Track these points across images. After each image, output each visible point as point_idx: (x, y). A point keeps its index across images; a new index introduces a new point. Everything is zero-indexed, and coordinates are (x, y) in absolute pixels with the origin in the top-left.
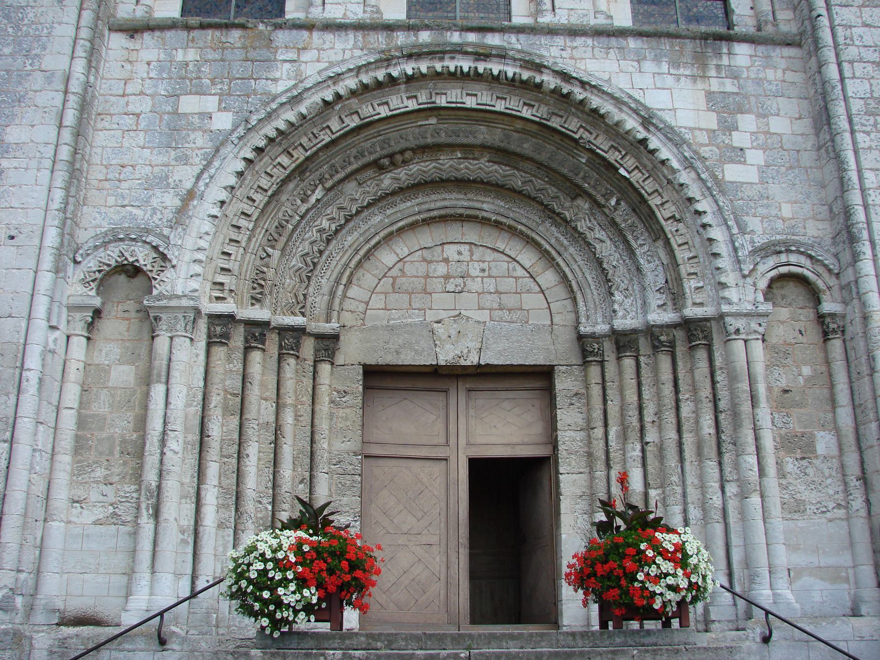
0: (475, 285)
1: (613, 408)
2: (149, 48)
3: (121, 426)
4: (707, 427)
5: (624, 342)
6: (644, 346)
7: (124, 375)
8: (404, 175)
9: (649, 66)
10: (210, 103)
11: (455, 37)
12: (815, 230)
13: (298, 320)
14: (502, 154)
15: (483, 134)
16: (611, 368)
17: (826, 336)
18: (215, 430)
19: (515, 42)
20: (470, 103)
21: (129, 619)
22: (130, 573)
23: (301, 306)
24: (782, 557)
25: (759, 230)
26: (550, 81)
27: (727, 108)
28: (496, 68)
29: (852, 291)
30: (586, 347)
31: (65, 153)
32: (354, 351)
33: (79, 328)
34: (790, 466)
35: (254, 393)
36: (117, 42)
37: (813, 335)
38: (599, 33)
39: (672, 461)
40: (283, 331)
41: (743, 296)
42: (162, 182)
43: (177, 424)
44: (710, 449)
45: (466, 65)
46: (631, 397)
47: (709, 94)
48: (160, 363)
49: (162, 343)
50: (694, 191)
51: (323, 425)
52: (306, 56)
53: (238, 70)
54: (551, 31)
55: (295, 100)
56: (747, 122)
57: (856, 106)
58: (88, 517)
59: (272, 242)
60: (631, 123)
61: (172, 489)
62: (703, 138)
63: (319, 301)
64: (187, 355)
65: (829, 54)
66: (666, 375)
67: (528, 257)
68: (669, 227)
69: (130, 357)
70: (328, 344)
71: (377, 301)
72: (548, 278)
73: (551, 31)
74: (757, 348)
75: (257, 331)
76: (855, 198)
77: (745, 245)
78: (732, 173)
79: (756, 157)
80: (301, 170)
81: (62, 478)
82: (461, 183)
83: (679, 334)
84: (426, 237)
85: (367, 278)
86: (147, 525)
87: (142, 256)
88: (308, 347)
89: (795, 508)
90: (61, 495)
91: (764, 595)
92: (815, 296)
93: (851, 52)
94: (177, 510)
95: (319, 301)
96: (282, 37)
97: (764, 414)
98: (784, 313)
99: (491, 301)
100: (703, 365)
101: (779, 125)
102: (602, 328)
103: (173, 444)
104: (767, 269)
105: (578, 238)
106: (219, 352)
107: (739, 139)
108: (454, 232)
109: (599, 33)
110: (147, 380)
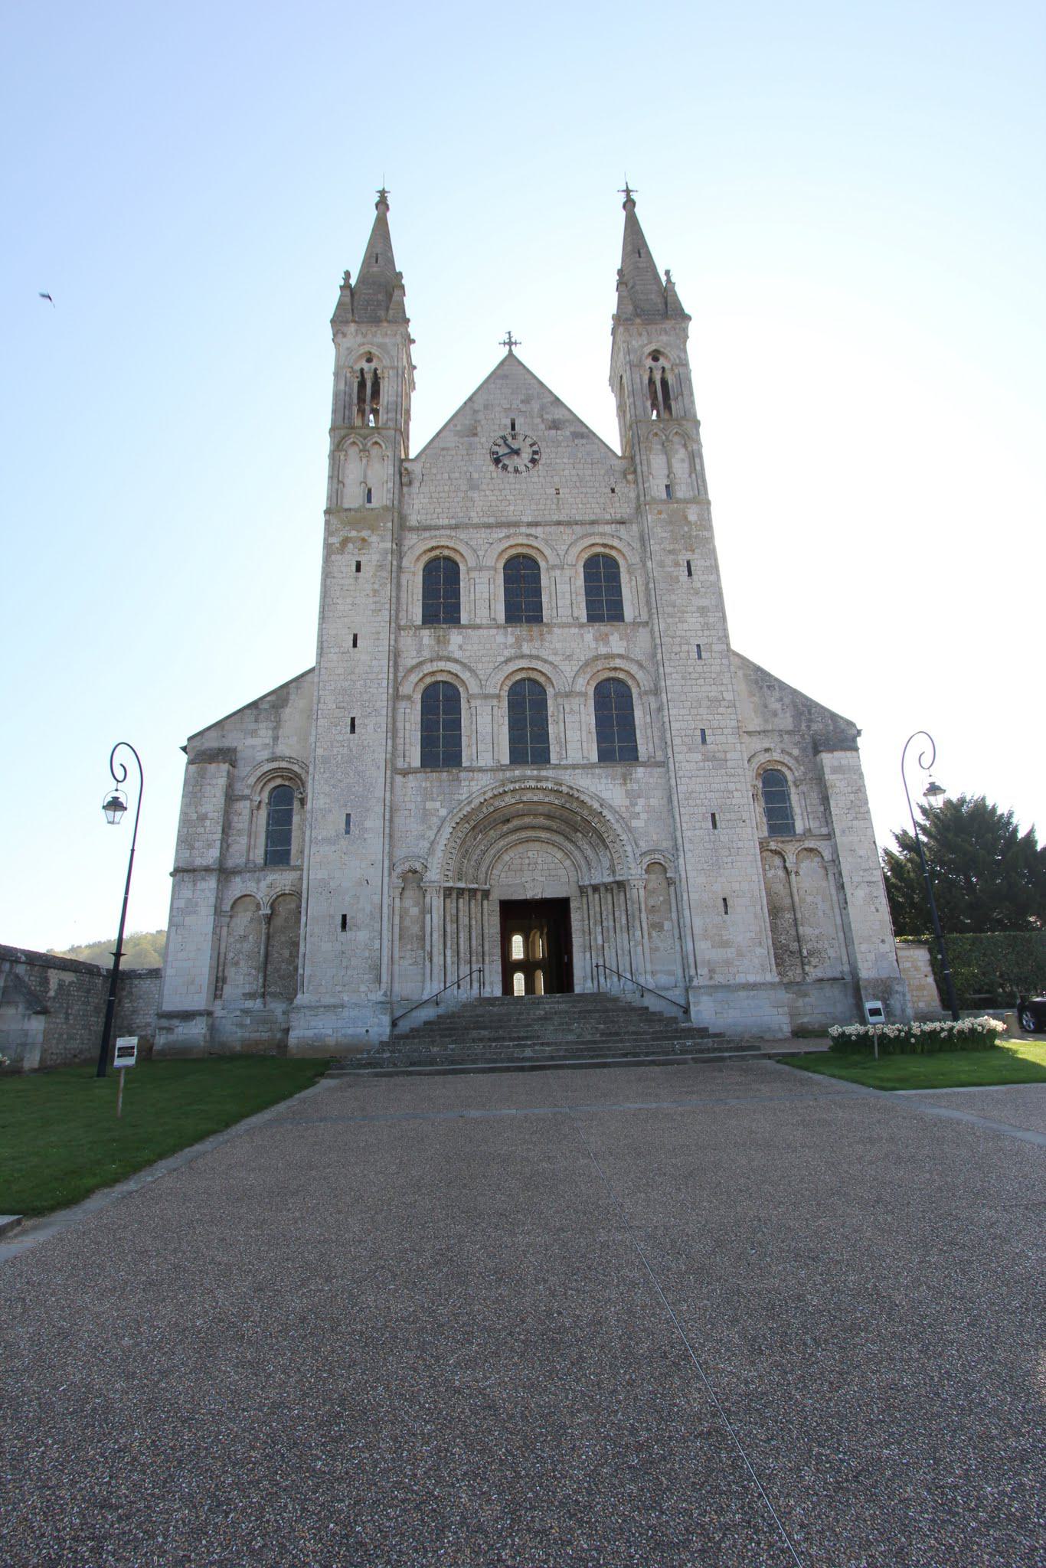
0: (540, 867)
1: (592, 913)
2: (412, 781)
3: (415, 929)
4: (624, 921)
5: (596, 888)
6: (602, 889)
7: (414, 911)
8: (510, 825)
9: (603, 781)
10: (438, 804)
11: (529, 773)
12: (666, 844)
13: (475, 886)
14: (548, 816)
15: (541, 809)
16: (591, 898)
17: (669, 885)
18: (448, 929)
19: (550, 773)
20: (535, 799)
21: (425, 997)
22: (423, 982)
23: (476, 880)
24: (649, 967)
25: (644, 846)
26: (565, 789)
28: (544, 785)
29: (677, 869)
30: (582, 890)
31: (387, 830)
32: (496, 895)
33: (397, 894)
34: (654, 934)
35: (461, 914)
36: (399, 778)
37: (665, 884)
38: (584, 767)
39: (612, 933)
40: (470, 890)
41: (633, 871)
42: (423, 837)
43: (435, 928)
44: (625, 930)
45: (533, 784)
46: (598, 909)
48: (428, 906)
49: (428, 899)
50: (620, 831)
51: (486, 924)
53: (447, 790)
54: (566, 767)
55: (470, 803)
56: (641, 801)
58: (406, 963)
59: (464, 857)
60: (596, 806)
61: (435, 950)
63: (482, 876)
64: (436, 902)
65: (672, 774)
66: (610, 901)
67: (559, 855)
68: (610, 845)
69: (417, 904)
70: (486, 894)
71: (503, 875)
72: (568, 863)
73: (566, 767)
74: (642, 892)
75: (461, 892)
76: (678, 834)
77: (638, 852)
78: (635, 823)
79: (644, 816)
80: (474, 828)
81: (396, 949)
82: (533, 828)
83: (615, 886)
84: (521, 848)
85: (499, 866)
86: (427, 963)
87: (418, 866)
88: (479, 896)
89: (654, 950)
90: (396, 956)
91: (642, 981)
92: (665, 870)
93: (680, 774)
94: (438, 959)
95: (482, 876)
96: (463, 775)
97: (644, 915)
98: (653, 877)
99: (546, 873)
100: (622, 898)
101: (654, 802)
102: (587, 883)
103: (435, 936)
104: (647, 860)
105: (578, 848)
106: (448, 901)
107: (638, 809)
108: (531, 844)
109: (584, 767)
110: (423, 912)
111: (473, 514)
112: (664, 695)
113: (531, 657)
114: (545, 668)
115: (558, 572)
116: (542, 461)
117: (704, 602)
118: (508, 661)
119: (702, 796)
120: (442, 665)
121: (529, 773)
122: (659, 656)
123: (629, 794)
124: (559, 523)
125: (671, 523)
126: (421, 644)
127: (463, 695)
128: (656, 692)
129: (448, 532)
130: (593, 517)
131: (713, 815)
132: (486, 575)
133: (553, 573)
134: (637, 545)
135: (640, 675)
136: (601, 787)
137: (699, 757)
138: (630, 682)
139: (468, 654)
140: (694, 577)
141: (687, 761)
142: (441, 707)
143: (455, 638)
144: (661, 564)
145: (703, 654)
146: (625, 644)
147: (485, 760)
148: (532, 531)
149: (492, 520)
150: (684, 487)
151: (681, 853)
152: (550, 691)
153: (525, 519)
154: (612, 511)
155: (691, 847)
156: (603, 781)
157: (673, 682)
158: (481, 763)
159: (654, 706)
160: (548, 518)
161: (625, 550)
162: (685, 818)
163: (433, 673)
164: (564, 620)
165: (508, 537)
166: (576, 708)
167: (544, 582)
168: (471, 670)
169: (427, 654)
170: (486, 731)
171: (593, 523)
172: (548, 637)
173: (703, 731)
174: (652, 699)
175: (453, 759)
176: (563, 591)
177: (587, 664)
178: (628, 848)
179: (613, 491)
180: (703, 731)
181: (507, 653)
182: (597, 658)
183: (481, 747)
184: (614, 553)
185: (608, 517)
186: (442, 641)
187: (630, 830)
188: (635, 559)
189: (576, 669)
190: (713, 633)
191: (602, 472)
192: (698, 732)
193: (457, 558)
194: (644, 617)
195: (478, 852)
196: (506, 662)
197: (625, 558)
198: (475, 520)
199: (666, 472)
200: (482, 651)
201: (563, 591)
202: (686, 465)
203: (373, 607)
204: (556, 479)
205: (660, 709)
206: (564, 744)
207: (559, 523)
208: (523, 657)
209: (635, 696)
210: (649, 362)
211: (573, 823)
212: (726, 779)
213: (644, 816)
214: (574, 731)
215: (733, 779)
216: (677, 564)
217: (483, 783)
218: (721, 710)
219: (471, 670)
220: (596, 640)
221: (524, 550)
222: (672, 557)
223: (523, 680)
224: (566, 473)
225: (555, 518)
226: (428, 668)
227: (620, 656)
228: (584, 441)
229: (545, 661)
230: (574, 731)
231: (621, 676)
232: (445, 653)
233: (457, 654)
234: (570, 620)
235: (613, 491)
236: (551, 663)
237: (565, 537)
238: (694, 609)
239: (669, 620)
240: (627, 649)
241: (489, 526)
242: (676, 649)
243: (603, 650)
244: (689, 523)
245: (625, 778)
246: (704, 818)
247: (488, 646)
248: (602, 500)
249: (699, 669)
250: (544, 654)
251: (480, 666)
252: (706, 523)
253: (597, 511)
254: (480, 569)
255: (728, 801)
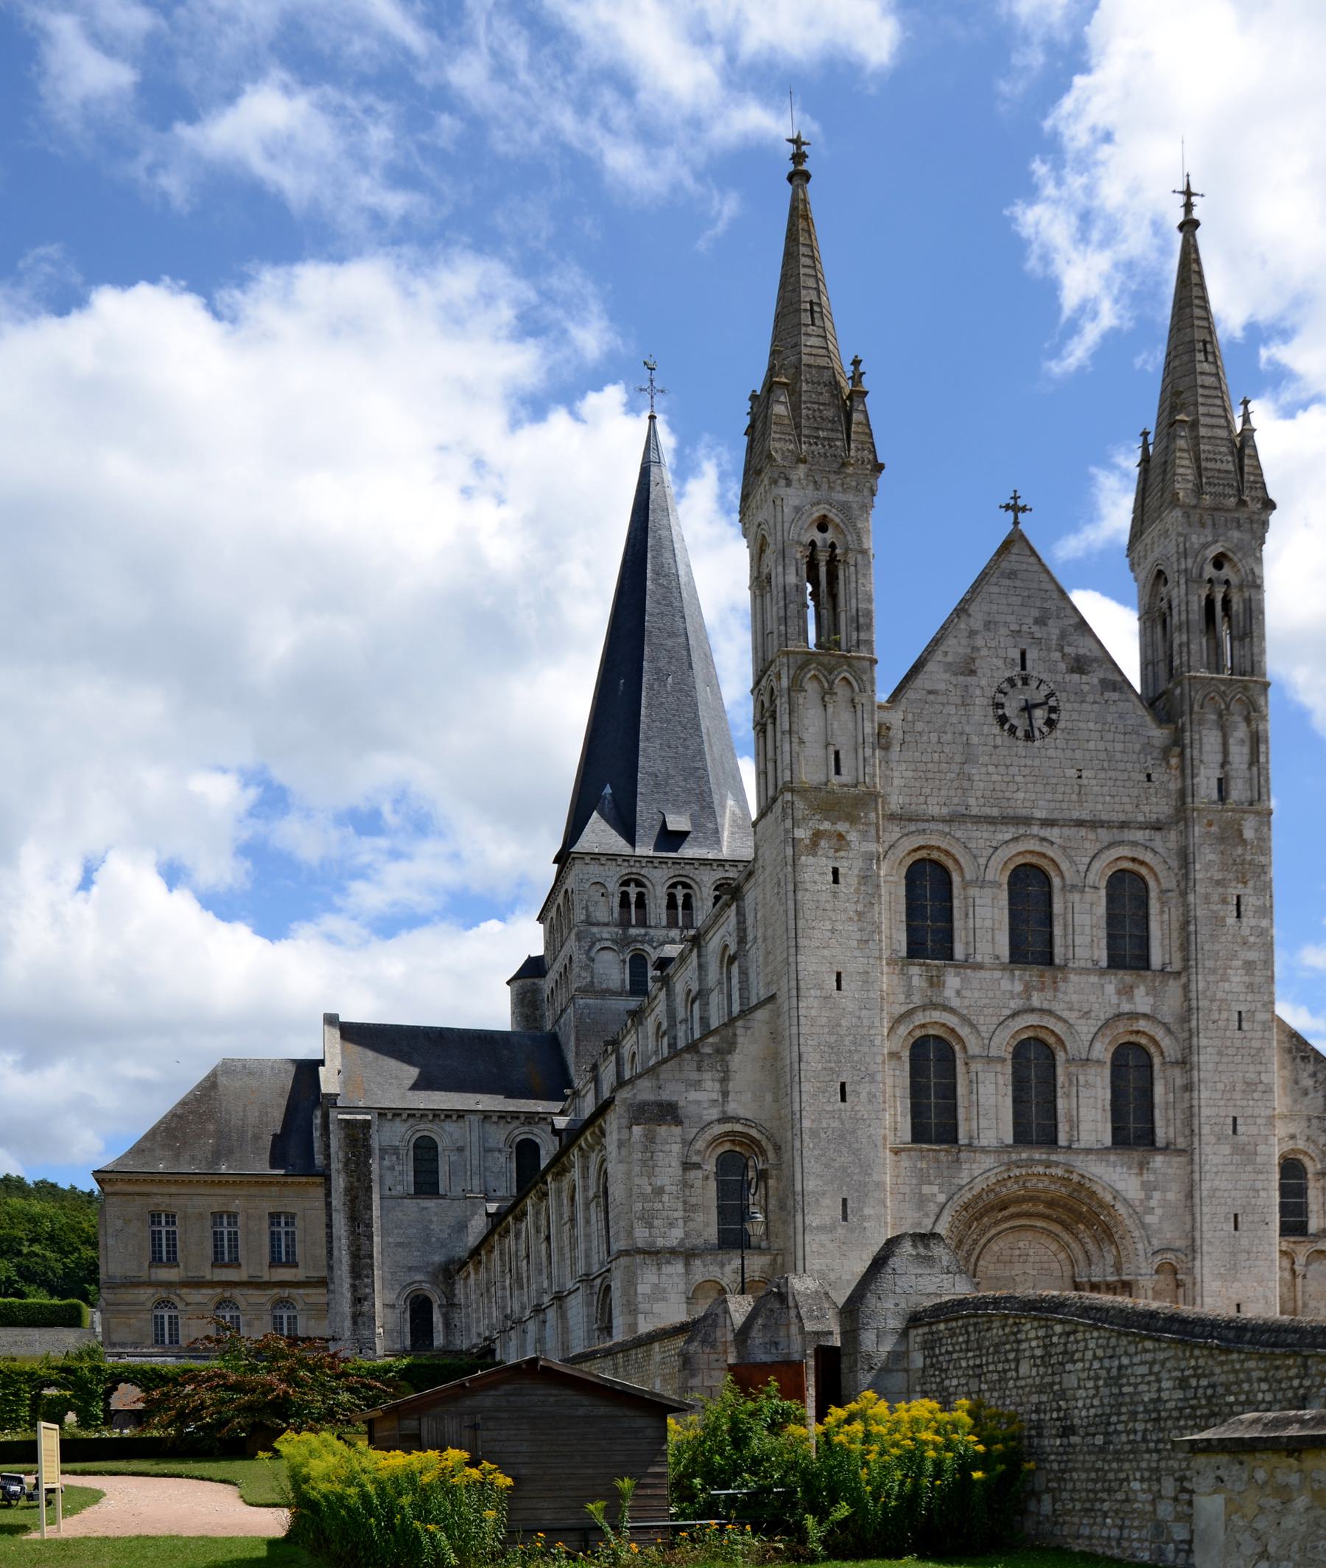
9: (1118, 1169)
17: (1178, 1286)
25: (1156, 1244)
27: (1148, 1188)
28: (1053, 1171)
45: (1041, 1169)
47: (1142, 1183)
50: (1132, 1228)
52: (974, 1166)
56: (1157, 1195)
57: (1205, 1193)
62: (1137, 1203)
65: (1196, 1168)
78: (1149, 1219)
79: (1159, 1211)
93: (1207, 1168)
101: (1170, 1196)
107: (1153, 1203)
111: (972, 801)
112: (1195, 1073)
113: (1042, 1011)
114: (1058, 1028)
115: (1077, 896)
116: (1061, 725)
117: (1252, 955)
118: (1015, 1015)
119: (1226, 1195)
120: (937, 1016)
121: (1037, 1156)
122: (1194, 1024)
123: (1144, 1185)
124: (1080, 823)
125: (1222, 839)
126: (910, 985)
127: (959, 1055)
128: (1184, 1063)
129: (941, 826)
130: (1122, 817)
131: (1236, 1216)
132: (988, 892)
133: (1070, 897)
134: (1174, 863)
135: (1166, 1042)
136: (1116, 1177)
137: (1226, 1149)
138: (1152, 1050)
139: (967, 1002)
140: (1244, 920)
141: (1213, 1154)
142: (933, 1065)
143: (952, 981)
144: (1207, 898)
145: (1245, 1025)
146: (1151, 1000)
147: (988, 1139)
148: (1046, 833)
149: (995, 812)
150: (1240, 782)
151: (1198, 1256)
152: (1061, 1057)
153: (1040, 814)
154: (1146, 809)
155: (1210, 1249)
156: (1118, 1169)
157: (1206, 1059)
158: (984, 1142)
159: (1179, 1082)
160: (1066, 815)
161: (1158, 868)
162: (1206, 1218)
163: (923, 1026)
164: (1082, 964)
165: (1015, 839)
166: (1091, 1079)
167: (1057, 908)
168: (972, 1026)
169: (917, 999)
170: (988, 1104)
171: (1124, 825)
172: (1062, 985)
173: (1235, 1119)
174: (1177, 1072)
175: (948, 1134)
176: (1082, 923)
177: (1107, 1024)
178: (1140, 1246)
179: (1149, 776)
180: (1235, 1119)
181: (1015, 1004)
182: (1119, 1016)
183: (983, 1123)
184: (1143, 871)
185: (1141, 819)
186: (935, 982)
187: (1144, 1226)
188: (1169, 881)
189: (1094, 1030)
190: (1257, 997)
191: (1137, 747)
192: (1230, 1121)
193: (950, 864)
194: (1177, 966)
195: (970, 1241)
196: (1015, 1015)
197: (1157, 880)
198: (975, 811)
199: (1219, 758)
200: (984, 999)
201: (1082, 923)
202: (1246, 750)
203: (858, 936)
204: (1078, 754)
205: (1189, 1087)
206: (1074, 1124)
207: (1080, 823)
208: (1033, 1010)
209: (1157, 1067)
210: (1209, 571)
211: (1079, 1214)
212: (1253, 1176)
213: (1159, 1211)
214: (1087, 1108)
215: (1261, 1177)
216: (1224, 901)
217: (986, 1166)
218: (1256, 1095)
219: (972, 1026)
220: (1119, 993)
221: (1034, 860)
222: (1221, 890)
223: (1029, 1038)
224: (1092, 745)
225: (1075, 815)
226: (919, 1018)
227: (1145, 1016)
228: (1116, 696)
229: (1060, 1018)
230: (1087, 1108)
231: (1143, 1041)
232: (939, 1000)
233: (955, 1003)
234: (1090, 965)
235: (1149, 776)
236: (1065, 1021)
237: (1087, 845)
238: (1240, 963)
239: (1211, 978)
240: (1154, 1007)
241: (991, 821)
242: (1216, 1016)
243: (1126, 1008)
244: (1244, 842)
245: (1142, 1166)
246: (1227, 1219)
247: (991, 994)
248: (1135, 792)
249: (1238, 1043)
250: (1057, 1008)
251: (982, 1021)
252: (1263, 845)
253: (1128, 808)
254: (982, 883)
255: (1253, 1201)
